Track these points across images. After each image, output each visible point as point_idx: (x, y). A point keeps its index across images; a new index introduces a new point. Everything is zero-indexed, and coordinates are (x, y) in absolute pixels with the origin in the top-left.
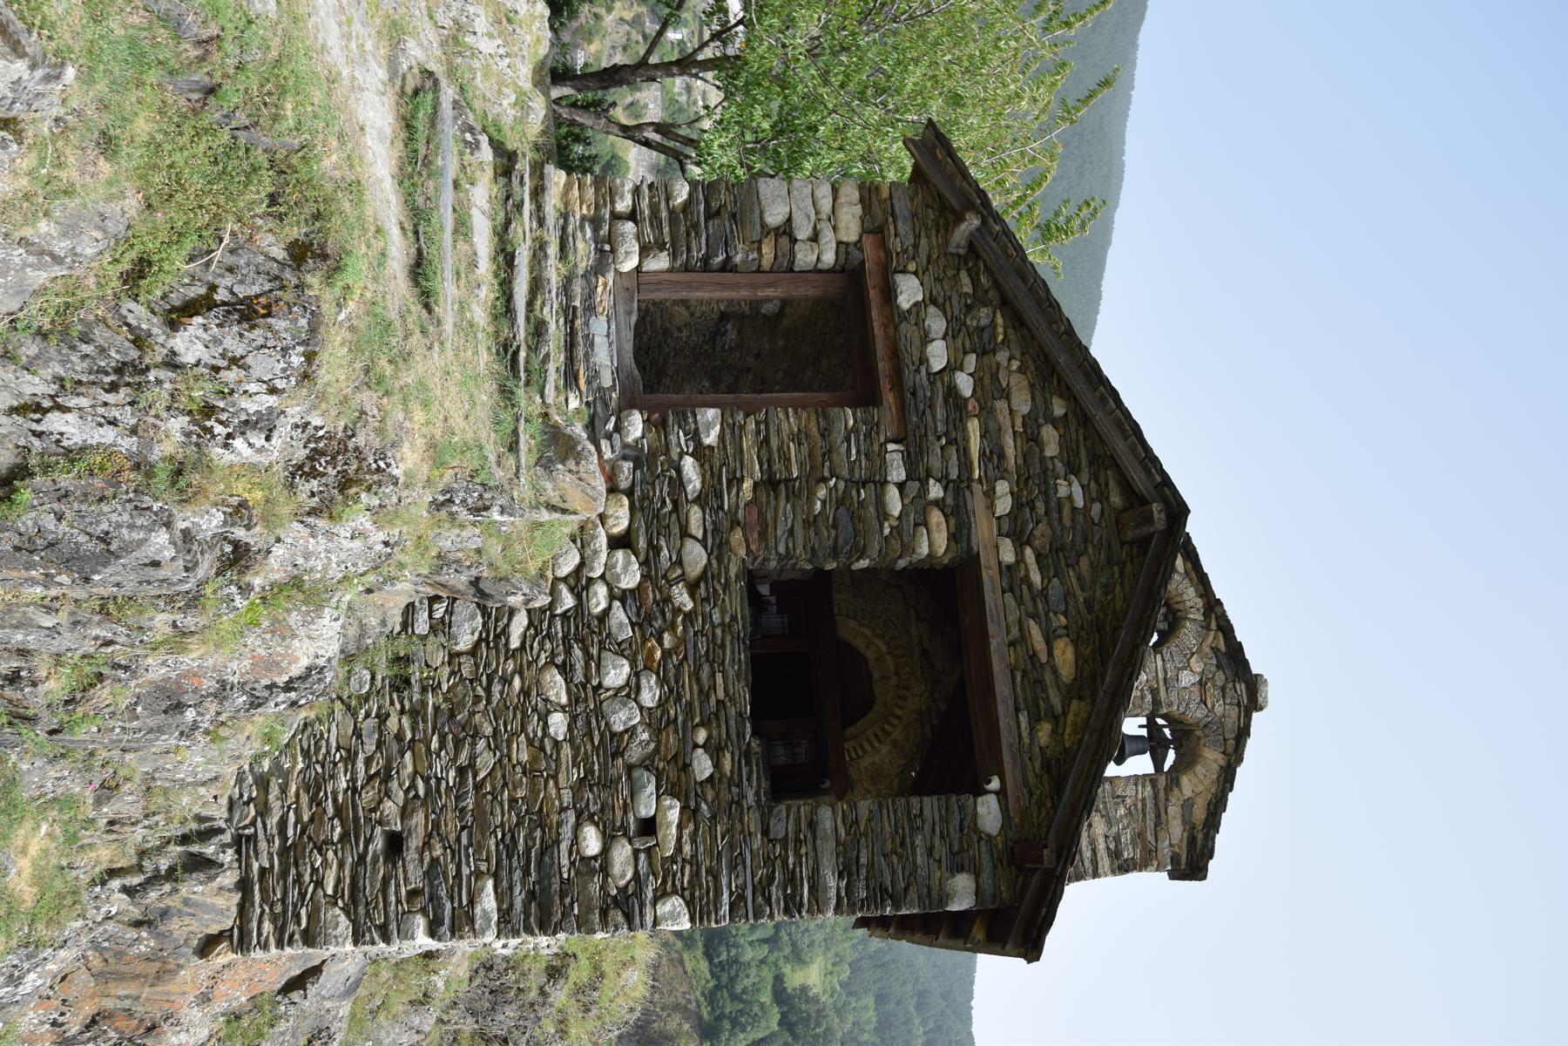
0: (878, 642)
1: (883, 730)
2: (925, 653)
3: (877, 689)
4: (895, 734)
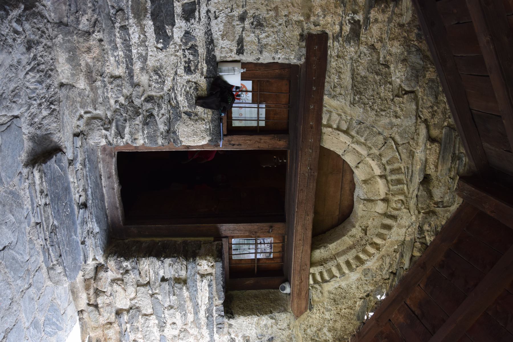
0: (374, 164)
1: (358, 258)
2: (426, 180)
3: (359, 208)
4: (369, 264)
